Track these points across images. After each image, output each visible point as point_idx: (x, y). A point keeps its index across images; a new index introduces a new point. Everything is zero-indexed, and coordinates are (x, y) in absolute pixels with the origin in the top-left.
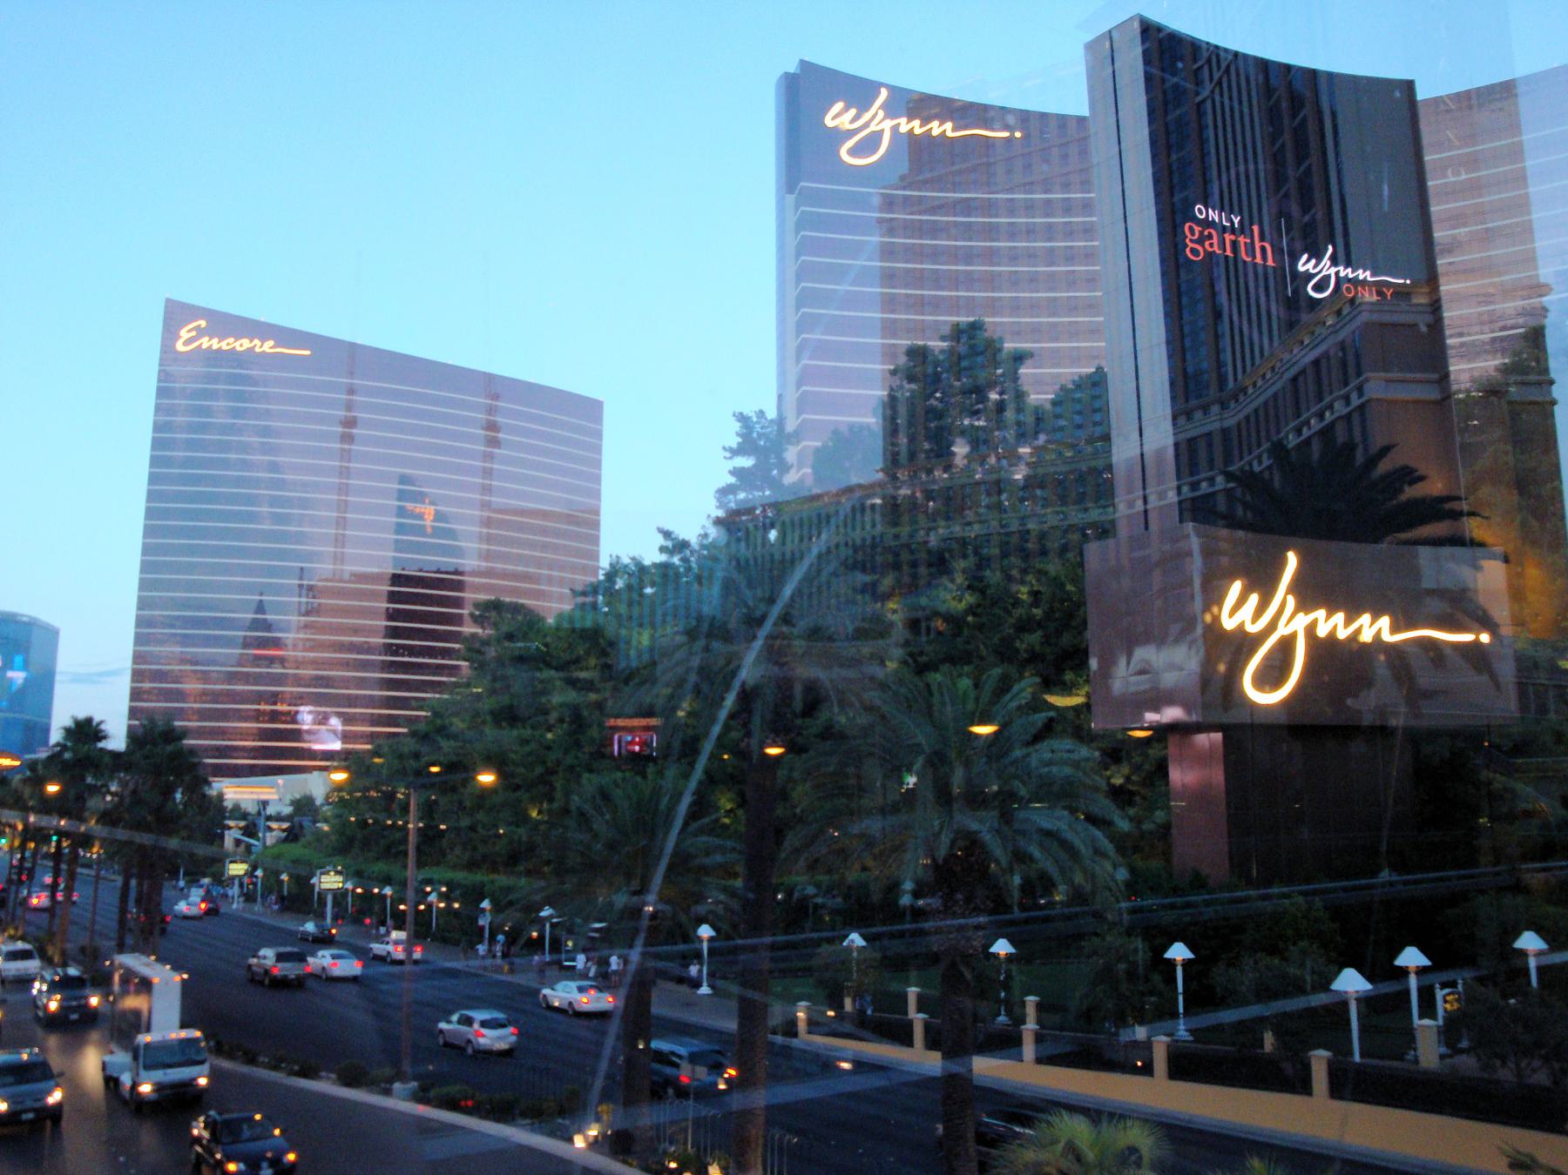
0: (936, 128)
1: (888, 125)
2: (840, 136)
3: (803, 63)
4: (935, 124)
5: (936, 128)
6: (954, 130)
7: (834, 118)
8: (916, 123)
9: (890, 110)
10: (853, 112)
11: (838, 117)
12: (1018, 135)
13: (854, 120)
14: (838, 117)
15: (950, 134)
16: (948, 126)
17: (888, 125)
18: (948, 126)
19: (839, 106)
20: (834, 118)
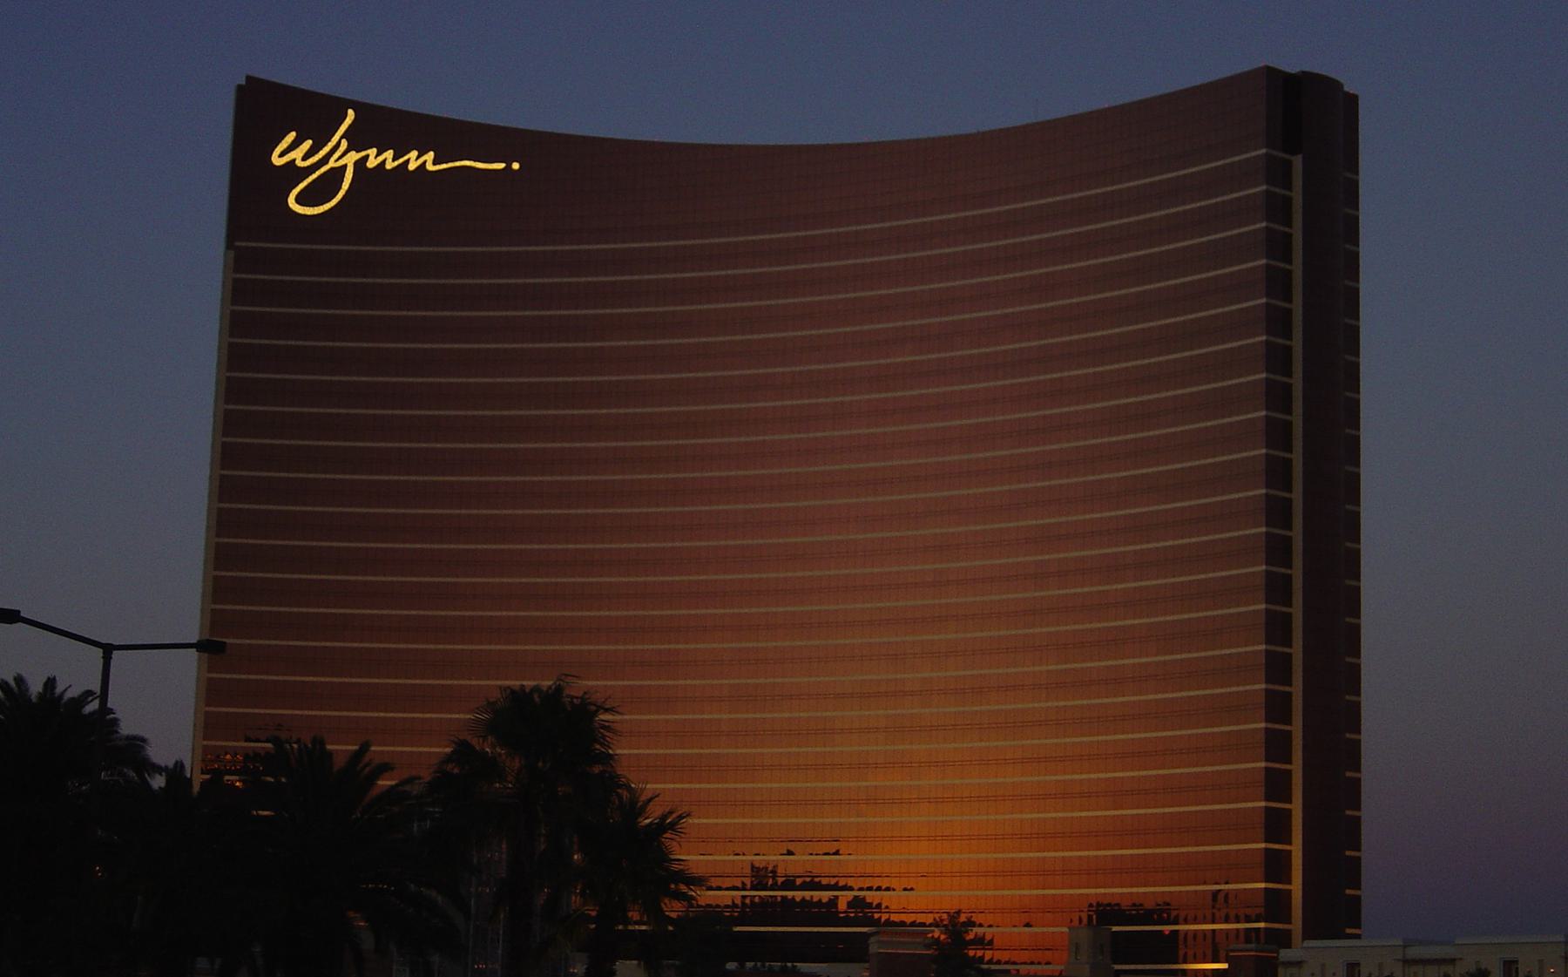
0: (413, 160)
1: (354, 156)
2: (293, 173)
3: (249, 78)
4: (414, 154)
5: (413, 160)
6: (434, 163)
7: (282, 155)
8: (389, 154)
9: (356, 140)
10: (308, 144)
11: (288, 152)
12: (516, 166)
13: (304, 159)
14: (288, 152)
15: (430, 167)
16: (430, 156)
17: (354, 156)
18: (430, 156)
19: (293, 135)
20: (282, 155)
